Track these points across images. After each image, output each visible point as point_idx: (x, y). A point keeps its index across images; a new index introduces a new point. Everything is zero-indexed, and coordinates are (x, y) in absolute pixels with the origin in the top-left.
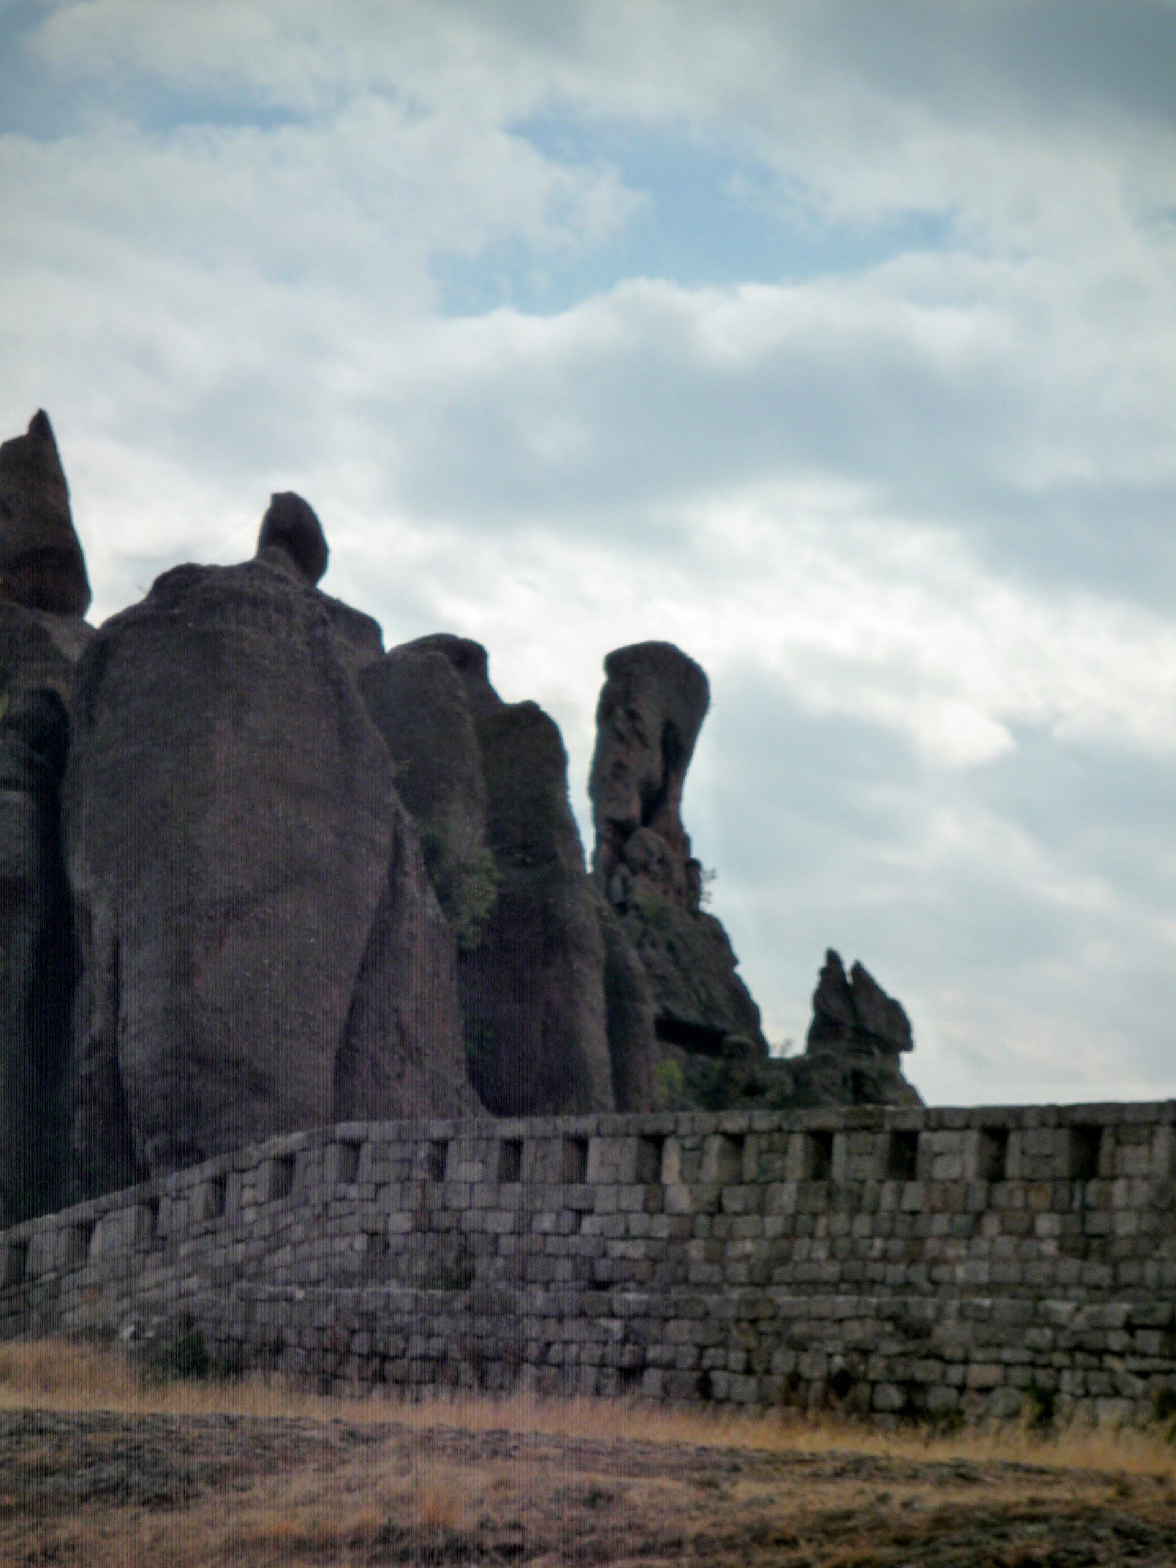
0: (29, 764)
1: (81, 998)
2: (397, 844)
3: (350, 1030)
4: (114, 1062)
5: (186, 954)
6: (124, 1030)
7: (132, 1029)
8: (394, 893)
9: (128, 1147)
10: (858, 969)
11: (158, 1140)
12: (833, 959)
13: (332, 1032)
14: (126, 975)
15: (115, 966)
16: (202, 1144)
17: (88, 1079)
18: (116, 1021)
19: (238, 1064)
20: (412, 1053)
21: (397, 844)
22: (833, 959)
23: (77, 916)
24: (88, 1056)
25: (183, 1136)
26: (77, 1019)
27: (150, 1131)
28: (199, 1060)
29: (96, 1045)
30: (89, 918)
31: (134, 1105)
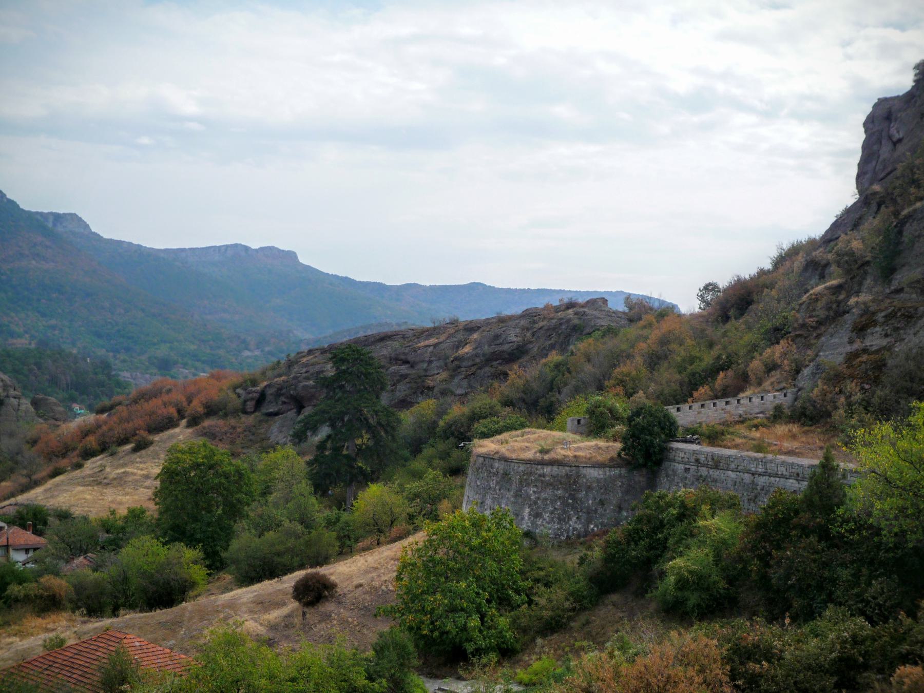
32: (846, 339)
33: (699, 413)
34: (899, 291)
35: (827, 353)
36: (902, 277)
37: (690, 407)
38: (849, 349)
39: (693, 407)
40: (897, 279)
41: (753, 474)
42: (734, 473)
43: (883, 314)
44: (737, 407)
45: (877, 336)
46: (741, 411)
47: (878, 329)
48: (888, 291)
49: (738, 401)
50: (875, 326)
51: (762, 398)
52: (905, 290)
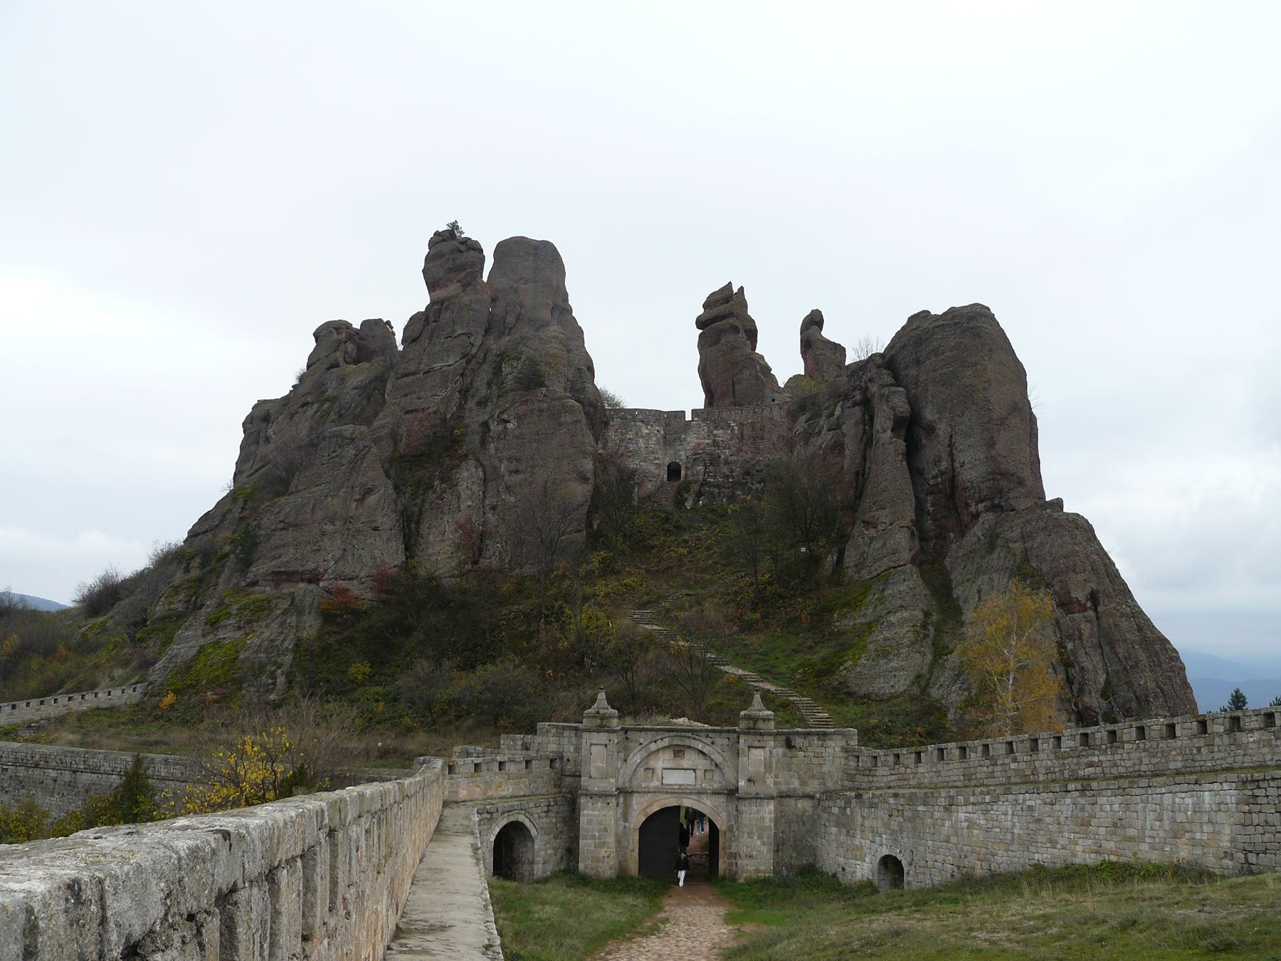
6: (962, 466)
11: (987, 503)
15: (951, 445)
16: (1003, 504)
19: (1012, 475)
25: (996, 502)
28: (1002, 474)
30: (931, 430)
32: (200, 632)
33: (37, 710)
34: (254, 584)
35: (180, 647)
36: (260, 569)
37: (28, 704)
38: (202, 641)
39: (31, 705)
40: (251, 572)
41: (74, 772)
42: (55, 771)
43: (236, 606)
44: (81, 703)
45: (229, 628)
47: (232, 621)
48: (243, 584)
49: (83, 696)
50: (228, 618)
51: (109, 693)
52: (260, 582)
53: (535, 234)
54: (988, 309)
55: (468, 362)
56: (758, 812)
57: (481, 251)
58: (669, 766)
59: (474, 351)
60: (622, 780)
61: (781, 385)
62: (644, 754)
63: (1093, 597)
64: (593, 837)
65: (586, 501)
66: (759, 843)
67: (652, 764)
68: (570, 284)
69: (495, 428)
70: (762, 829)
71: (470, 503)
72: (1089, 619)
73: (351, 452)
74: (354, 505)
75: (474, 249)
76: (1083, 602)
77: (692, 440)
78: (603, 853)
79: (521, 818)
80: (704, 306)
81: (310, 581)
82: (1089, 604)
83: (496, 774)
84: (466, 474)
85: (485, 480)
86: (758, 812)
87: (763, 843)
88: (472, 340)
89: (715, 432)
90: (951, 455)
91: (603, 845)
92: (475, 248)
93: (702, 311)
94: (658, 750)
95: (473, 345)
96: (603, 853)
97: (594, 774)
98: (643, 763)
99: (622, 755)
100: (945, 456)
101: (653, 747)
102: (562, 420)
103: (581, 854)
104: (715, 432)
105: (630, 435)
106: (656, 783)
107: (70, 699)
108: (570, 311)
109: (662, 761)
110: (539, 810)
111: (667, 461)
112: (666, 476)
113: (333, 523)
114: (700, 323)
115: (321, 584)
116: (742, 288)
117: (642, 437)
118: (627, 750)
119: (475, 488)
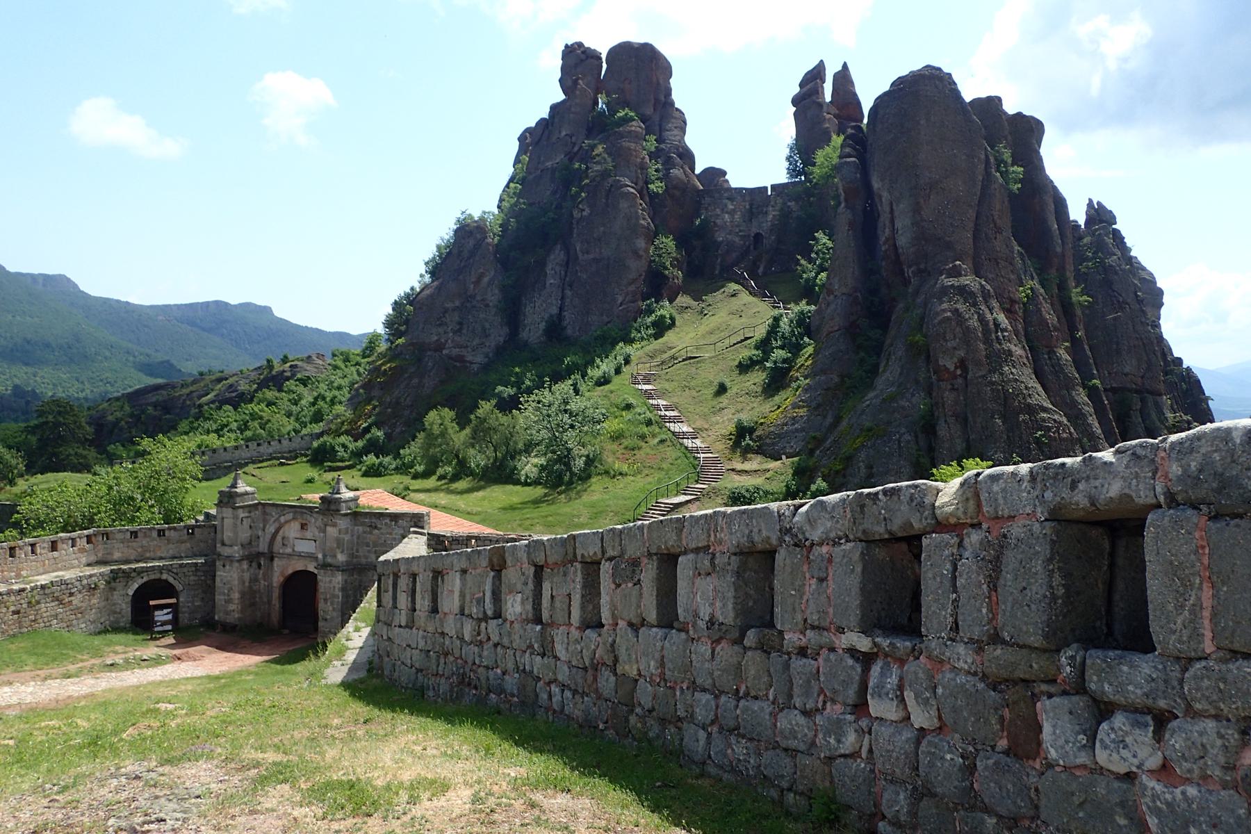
0: (854, 149)
1: (880, 225)
2: (987, 156)
3: (976, 225)
4: (895, 245)
5: (918, 203)
7: (900, 232)
8: (988, 173)
9: (902, 272)
10: (1099, 203)
12: (1091, 201)
13: (972, 225)
14: (896, 214)
17: (886, 251)
18: (894, 230)
19: (939, 239)
20: (999, 230)
21: (987, 156)
22: (1091, 201)
23: (877, 200)
24: (884, 244)
25: (922, 266)
26: (879, 232)
27: (910, 267)
29: (887, 240)
30: (880, 197)
31: (902, 258)
46: (271, 450)
53: (637, 38)
54: (939, 69)
55: (571, 160)
56: (330, 582)
57: (601, 59)
58: (298, 536)
59: (576, 149)
60: (263, 547)
61: (698, 171)
62: (277, 525)
63: (962, 364)
64: (224, 594)
65: (641, 275)
66: (331, 608)
67: (287, 534)
68: (673, 82)
69: (576, 214)
70: (334, 596)
71: (552, 281)
72: (956, 386)
73: (471, 242)
74: (472, 286)
75: (592, 57)
76: (952, 368)
77: (772, 214)
78: (232, 607)
79: (164, 576)
80: (801, 85)
81: (436, 350)
82: (959, 372)
83: (154, 539)
84: (552, 257)
85: (567, 263)
86: (330, 582)
87: (334, 609)
88: (574, 139)
89: (789, 204)
90: (892, 221)
91: (229, 601)
92: (597, 57)
93: (798, 89)
94: (286, 522)
95: (574, 144)
96: (232, 607)
97: (227, 542)
98: (281, 532)
99: (261, 525)
100: (887, 223)
101: (282, 519)
102: (621, 205)
103: (217, 610)
104: (789, 204)
105: (718, 211)
106: (289, 550)
107: (259, 445)
108: (672, 104)
109: (292, 530)
110: (185, 570)
111: (754, 230)
112: (752, 247)
113: (453, 302)
114: (796, 101)
115: (444, 352)
116: (845, 66)
117: (727, 213)
118: (265, 522)
119: (558, 269)
